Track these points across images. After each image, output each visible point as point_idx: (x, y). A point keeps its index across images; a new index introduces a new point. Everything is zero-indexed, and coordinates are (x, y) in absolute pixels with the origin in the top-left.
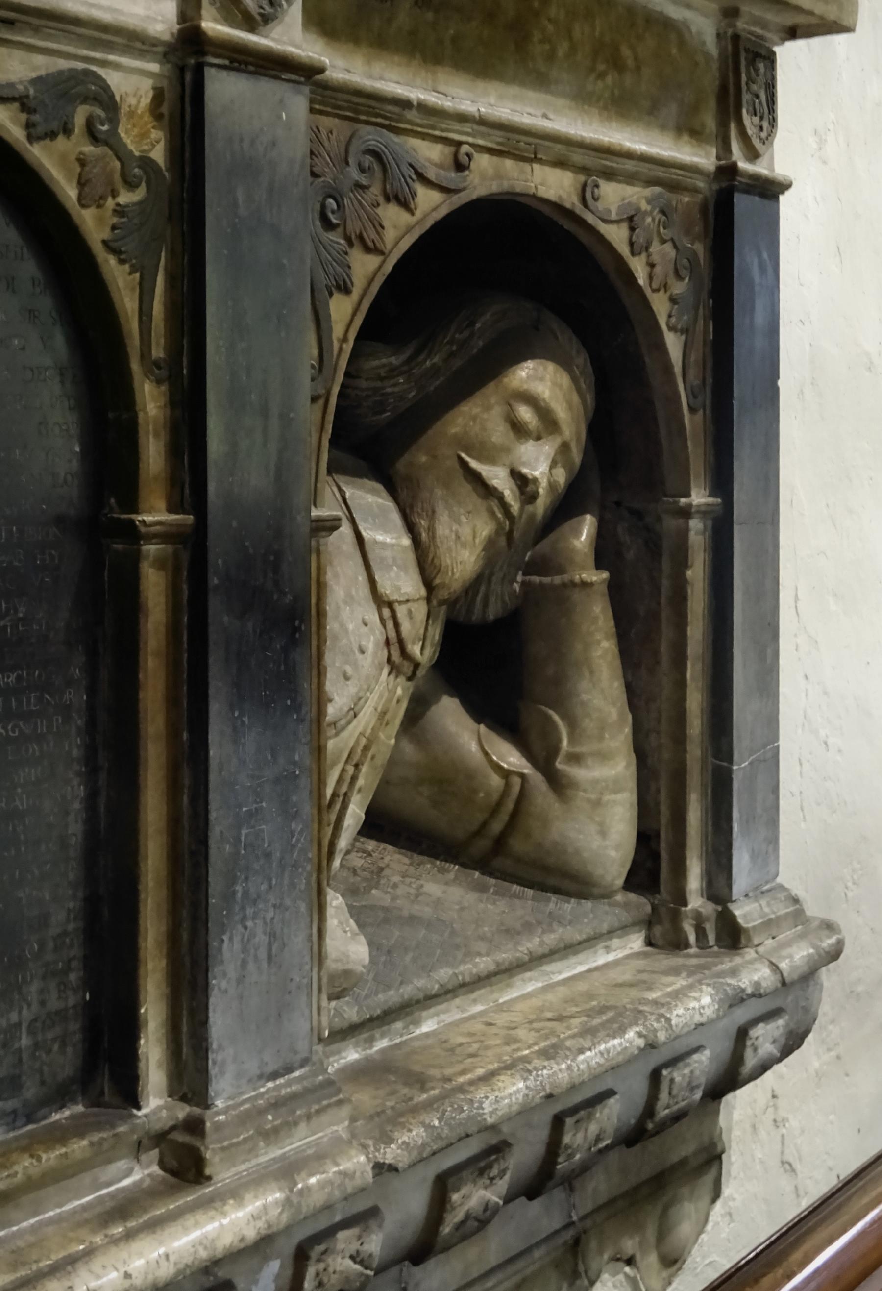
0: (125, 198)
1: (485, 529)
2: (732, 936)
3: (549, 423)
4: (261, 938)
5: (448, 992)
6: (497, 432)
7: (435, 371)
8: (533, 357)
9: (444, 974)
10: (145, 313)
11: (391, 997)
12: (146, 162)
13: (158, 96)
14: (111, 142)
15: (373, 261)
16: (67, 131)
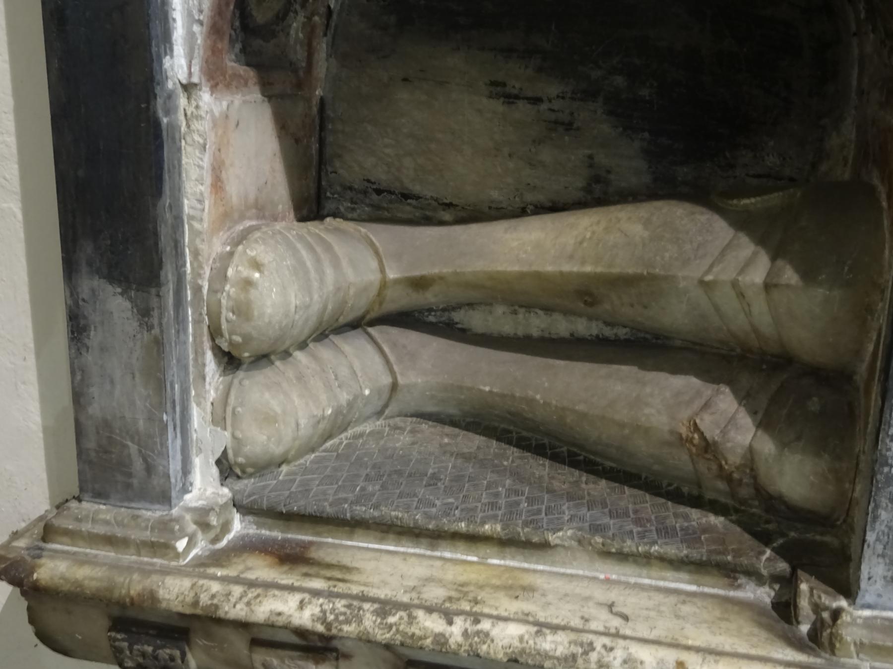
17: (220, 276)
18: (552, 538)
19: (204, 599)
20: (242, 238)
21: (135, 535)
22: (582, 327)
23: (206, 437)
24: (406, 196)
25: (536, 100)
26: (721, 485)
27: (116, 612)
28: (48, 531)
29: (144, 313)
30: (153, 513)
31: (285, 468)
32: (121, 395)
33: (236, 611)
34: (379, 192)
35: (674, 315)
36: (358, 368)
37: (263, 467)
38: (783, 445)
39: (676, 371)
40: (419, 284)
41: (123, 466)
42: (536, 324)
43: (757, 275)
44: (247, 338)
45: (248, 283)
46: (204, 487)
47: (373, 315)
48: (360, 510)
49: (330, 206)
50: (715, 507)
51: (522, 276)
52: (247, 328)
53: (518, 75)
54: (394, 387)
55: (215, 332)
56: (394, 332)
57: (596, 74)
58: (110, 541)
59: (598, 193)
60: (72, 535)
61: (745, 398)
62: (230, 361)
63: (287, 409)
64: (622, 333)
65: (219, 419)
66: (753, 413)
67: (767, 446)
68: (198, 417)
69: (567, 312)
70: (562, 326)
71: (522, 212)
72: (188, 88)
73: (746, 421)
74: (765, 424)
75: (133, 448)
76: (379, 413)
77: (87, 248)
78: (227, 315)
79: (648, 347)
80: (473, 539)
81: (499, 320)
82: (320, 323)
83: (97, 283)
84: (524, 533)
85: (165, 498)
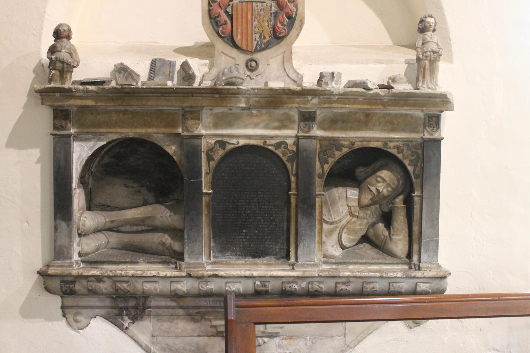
0: (289, 155)
1: (370, 197)
2: (419, 269)
3: (384, 180)
4: (306, 244)
5: (357, 263)
6: (374, 182)
7: (369, 172)
8: (388, 170)
9: (354, 261)
10: (292, 168)
11: (342, 261)
12: (292, 151)
13: (294, 142)
14: (287, 148)
15: (333, 159)
16: (281, 148)
17: (79, 219)
18: (139, 261)
19: (80, 273)
20: (82, 213)
21: (66, 265)
22: (144, 228)
23: (76, 249)
24: (108, 206)
25: (133, 187)
26: (167, 251)
27: (62, 279)
28: (48, 266)
29: (68, 225)
30: (69, 261)
31: (89, 256)
32: (63, 240)
33: (86, 274)
34: (102, 206)
35: (157, 223)
36: (101, 239)
37: (87, 254)
38: (174, 241)
39: (159, 233)
40: (112, 222)
41: (63, 253)
42: (135, 228)
43: (168, 215)
44: (84, 230)
45: (84, 221)
46: (76, 257)
47: (103, 228)
48: (105, 260)
49: (92, 209)
50: (167, 256)
51: (131, 218)
52: (85, 228)
53: (129, 183)
54: (108, 242)
55: (78, 229)
56: (107, 232)
57: (144, 182)
58: (61, 266)
59: (145, 203)
60: (54, 266)
61: (169, 235)
62: (80, 235)
63: (90, 244)
64: (150, 228)
65: (79, 245)
66: (170, 237)
67: (172, 242)
68: (75, 245)
69: (141, 225)
70: (140, 228)
71: (132, 208)
72: (75, 189)
73: (169, 239)
74: (172, 238)
75: (65, 250)
76: (105, 248)
77: (59, 215)
78: (81, 226)
79: (155, 229)
80: (125, 263)
81: (128, 228)
82: (98, 227)
83: (60, 221)
84: (134, 260)
85: (71, 258)
